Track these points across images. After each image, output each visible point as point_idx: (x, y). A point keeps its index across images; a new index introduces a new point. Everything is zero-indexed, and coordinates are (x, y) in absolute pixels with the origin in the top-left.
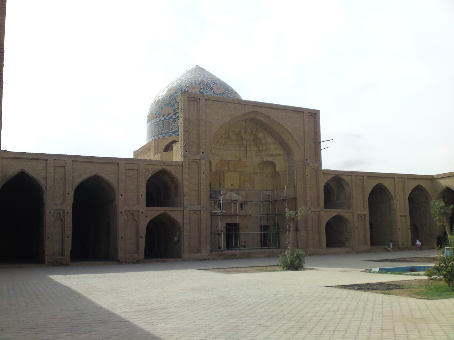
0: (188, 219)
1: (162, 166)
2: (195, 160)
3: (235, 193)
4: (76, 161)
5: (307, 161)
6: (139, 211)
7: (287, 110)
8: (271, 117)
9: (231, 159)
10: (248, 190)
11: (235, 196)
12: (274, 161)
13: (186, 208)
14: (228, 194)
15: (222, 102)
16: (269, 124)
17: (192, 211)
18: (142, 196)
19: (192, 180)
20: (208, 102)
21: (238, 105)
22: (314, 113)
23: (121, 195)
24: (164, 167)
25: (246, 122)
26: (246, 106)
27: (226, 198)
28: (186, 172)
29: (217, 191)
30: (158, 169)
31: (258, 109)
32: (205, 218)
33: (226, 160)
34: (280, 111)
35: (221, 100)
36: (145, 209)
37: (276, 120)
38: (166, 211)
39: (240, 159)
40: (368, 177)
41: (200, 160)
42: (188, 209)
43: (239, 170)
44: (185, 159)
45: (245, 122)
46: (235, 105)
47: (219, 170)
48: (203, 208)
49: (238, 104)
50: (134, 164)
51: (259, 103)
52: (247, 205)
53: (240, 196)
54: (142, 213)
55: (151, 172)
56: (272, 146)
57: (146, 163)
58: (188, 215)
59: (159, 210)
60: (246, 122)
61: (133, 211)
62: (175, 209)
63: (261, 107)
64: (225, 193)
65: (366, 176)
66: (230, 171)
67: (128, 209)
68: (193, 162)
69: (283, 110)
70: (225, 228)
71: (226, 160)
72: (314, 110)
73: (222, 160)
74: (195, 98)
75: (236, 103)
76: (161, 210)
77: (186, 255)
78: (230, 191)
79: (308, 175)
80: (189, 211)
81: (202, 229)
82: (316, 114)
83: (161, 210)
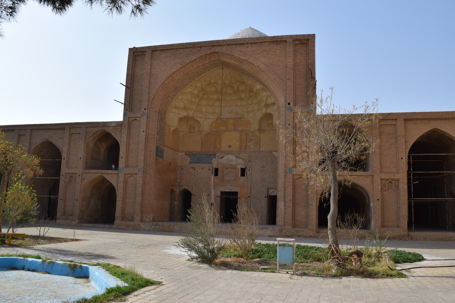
0: (122, 183)
1: (102, 128)
2: (136, 119)
3: (234, 156)
4: (34, 129)
5: (289, 106)
6: (76, 173)
7: (260, 42)
8: (236, 55)
9: (231, 116)
10: (252, 152)
11: (231, 159)
12: (272, 113)
13: (121, 170)
14: (226, 157)
15: (171, 49)
16: (239, 65)
17: (129, 174)
18: (80, 158)
19: (132, 140)
20: (157, 52)
21: (191, 49)
22: (304, 40)
23: (64, 158)
24: (104, 128)
25: (223, 69)
26: (202, 48)
27: (222, 162)
28: (124, 132)
29: (211, 154)
30: (99, 131)
31: (217, 49)
32: (141, 182)
33: (224, 119)
34: (249, 45)
35: (170, 48)
36: (82, 172)
37: (242, 58)
38: (102, 175)
39: (243, 116)
40: (405, 120)
41: (141, 117)
42: (123, 172)
43: (239, 129)
44: (125, 117)
45: (222, 69)
46: (187, 50)
47: (215, 130)
48: (140, 170)
49: (191, 48)
50: (77, 127)
51: (218, 41)
52: (250, 170)
53: (241, 159)
54: (80, 175)
55: (92, 134)
56: (264, 94)
57: (87, 126)
58: (122, 178)
59: (96, 173)
60: (223, 69)
61: (73, 173)
62: (110, 171)
63: (221, 45)
64: (222, 156)
65: (403, 120)
66: (228, 131)
67: (68, 171)
68: (136, 121)
69: (254, 43)
70: (219, 198)
71: (224, 119)
72: (303, 36)
73: (217, 119)
74: (142, 52)
75: (188, 48)
76: (97, 173)
77: (117, 221)
78: (228, 154)
79: (289, 125)
80: (125, 174)
81: (137, 195)
82: (308, 40)
83: (97, 173)
